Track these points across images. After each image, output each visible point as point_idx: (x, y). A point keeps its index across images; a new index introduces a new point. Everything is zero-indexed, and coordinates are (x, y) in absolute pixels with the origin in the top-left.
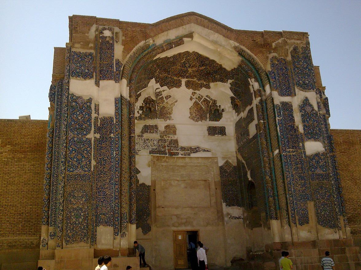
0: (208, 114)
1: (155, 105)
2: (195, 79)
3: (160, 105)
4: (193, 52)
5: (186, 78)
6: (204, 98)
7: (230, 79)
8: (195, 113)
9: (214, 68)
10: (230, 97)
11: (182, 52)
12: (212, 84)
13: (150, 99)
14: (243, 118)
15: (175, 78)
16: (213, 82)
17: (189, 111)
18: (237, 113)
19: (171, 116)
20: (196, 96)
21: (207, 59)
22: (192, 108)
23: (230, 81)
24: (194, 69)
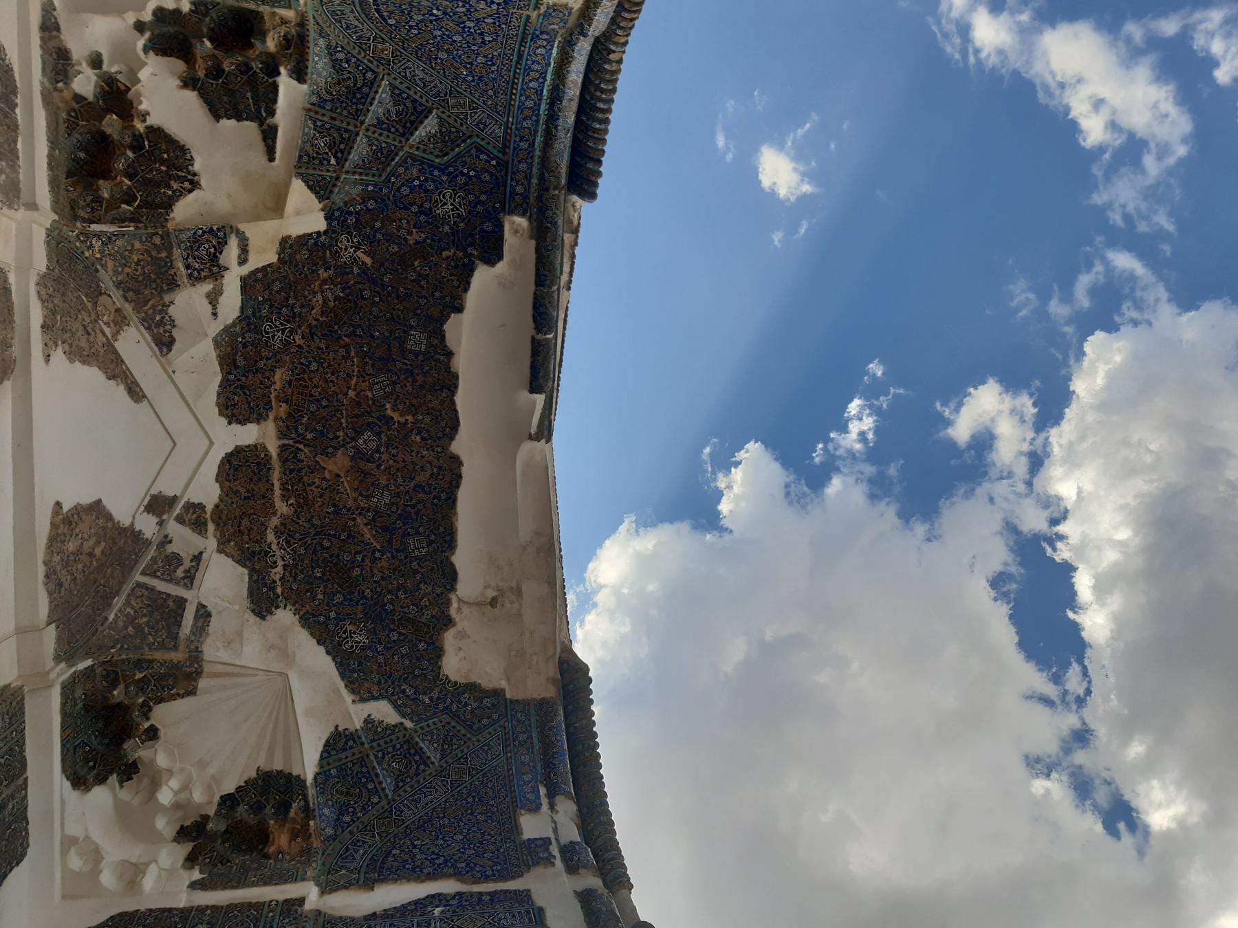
0: (89, 662)
1: (121, 220)
2: (282, 507)
3: (110, 264)
4: (456, 461)
5: (283, 449)
6: (181, 603)
7: (397, 707)
8: (79, 552)
9: (401, 595)
10: (278, 766)
11: (460, 399)
12: (285, 617)
13: (175, 185)
14: (308, 906)
15: (280, 376)
16: (308, 621)
17: (86, 500)
18: (196, 875)
19: (60, 351)
20: (184, 540)
21: (448, 541)
22: (101, 522)
23: (383, 711)
24: (346, 484)
